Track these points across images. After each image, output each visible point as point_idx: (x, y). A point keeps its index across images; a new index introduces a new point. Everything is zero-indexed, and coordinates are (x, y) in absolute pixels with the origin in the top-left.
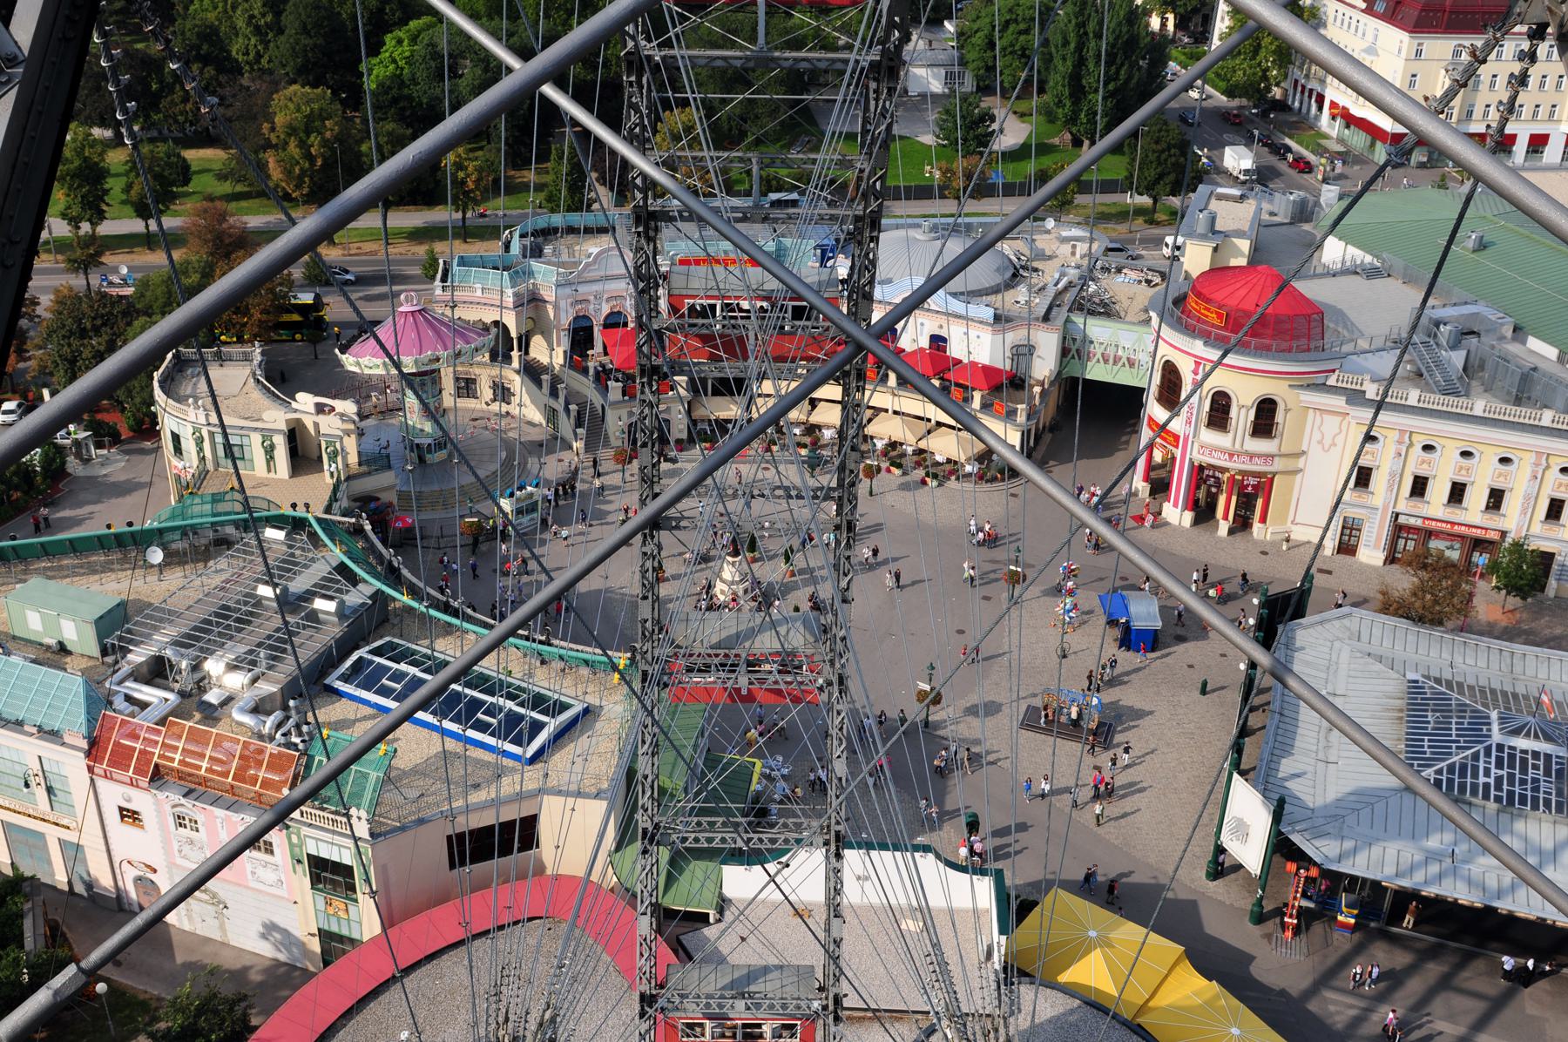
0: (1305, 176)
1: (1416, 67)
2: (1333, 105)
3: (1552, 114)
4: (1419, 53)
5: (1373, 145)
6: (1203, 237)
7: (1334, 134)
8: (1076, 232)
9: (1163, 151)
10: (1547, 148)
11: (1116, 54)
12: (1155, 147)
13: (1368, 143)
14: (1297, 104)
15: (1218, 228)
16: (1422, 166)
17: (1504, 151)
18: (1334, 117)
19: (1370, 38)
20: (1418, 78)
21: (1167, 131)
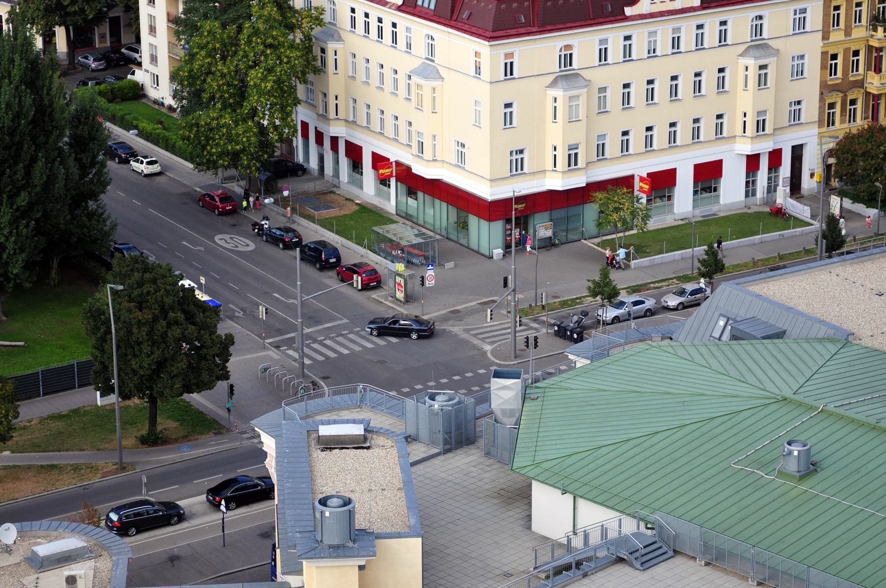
0: (374, 295)
1: (510, 91)
2: (379, 161)
3: (719, 129)
4: (509, 69)
5: (463, 226)
6: (338, 551)
7: (390, 206)
8: (71, 543)
9: (155, 320)
10: (723, 181)
11: (20, 144)
12: (139, 315)
13: (453, 217)
14: (313, 164)
15: (360, 522)
16: (548, 244)
17: (661, 197)
18: (384, 181)
19: (420, 48)
20: (514, 109)
21: (154, 281)
